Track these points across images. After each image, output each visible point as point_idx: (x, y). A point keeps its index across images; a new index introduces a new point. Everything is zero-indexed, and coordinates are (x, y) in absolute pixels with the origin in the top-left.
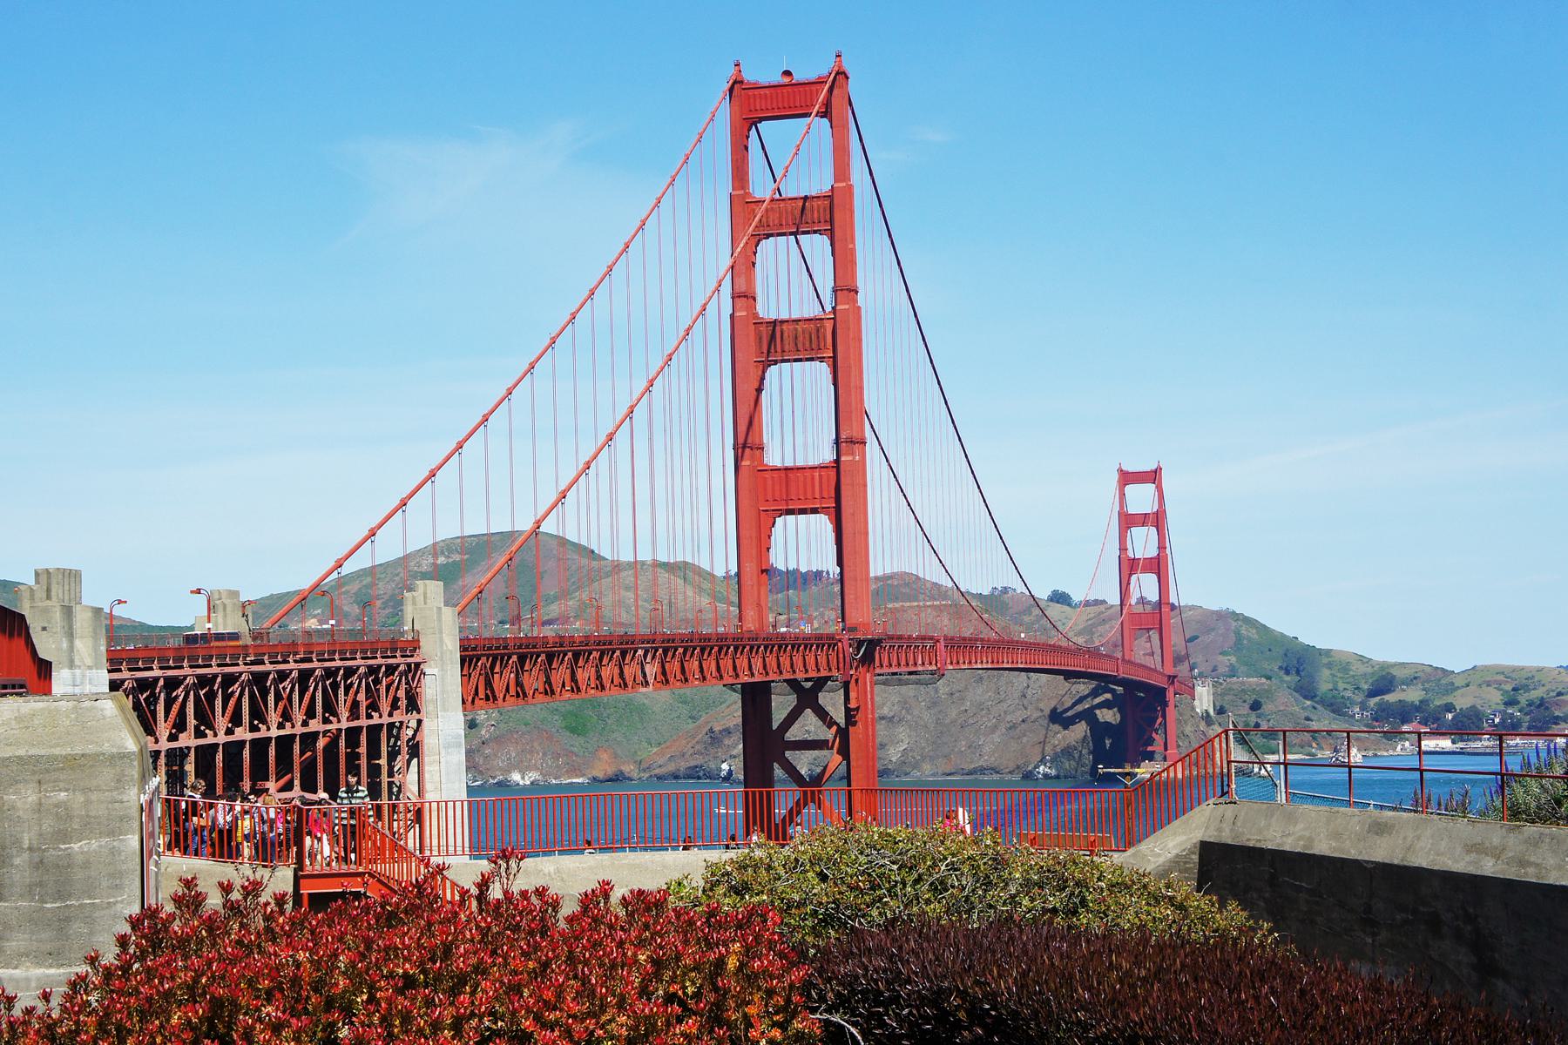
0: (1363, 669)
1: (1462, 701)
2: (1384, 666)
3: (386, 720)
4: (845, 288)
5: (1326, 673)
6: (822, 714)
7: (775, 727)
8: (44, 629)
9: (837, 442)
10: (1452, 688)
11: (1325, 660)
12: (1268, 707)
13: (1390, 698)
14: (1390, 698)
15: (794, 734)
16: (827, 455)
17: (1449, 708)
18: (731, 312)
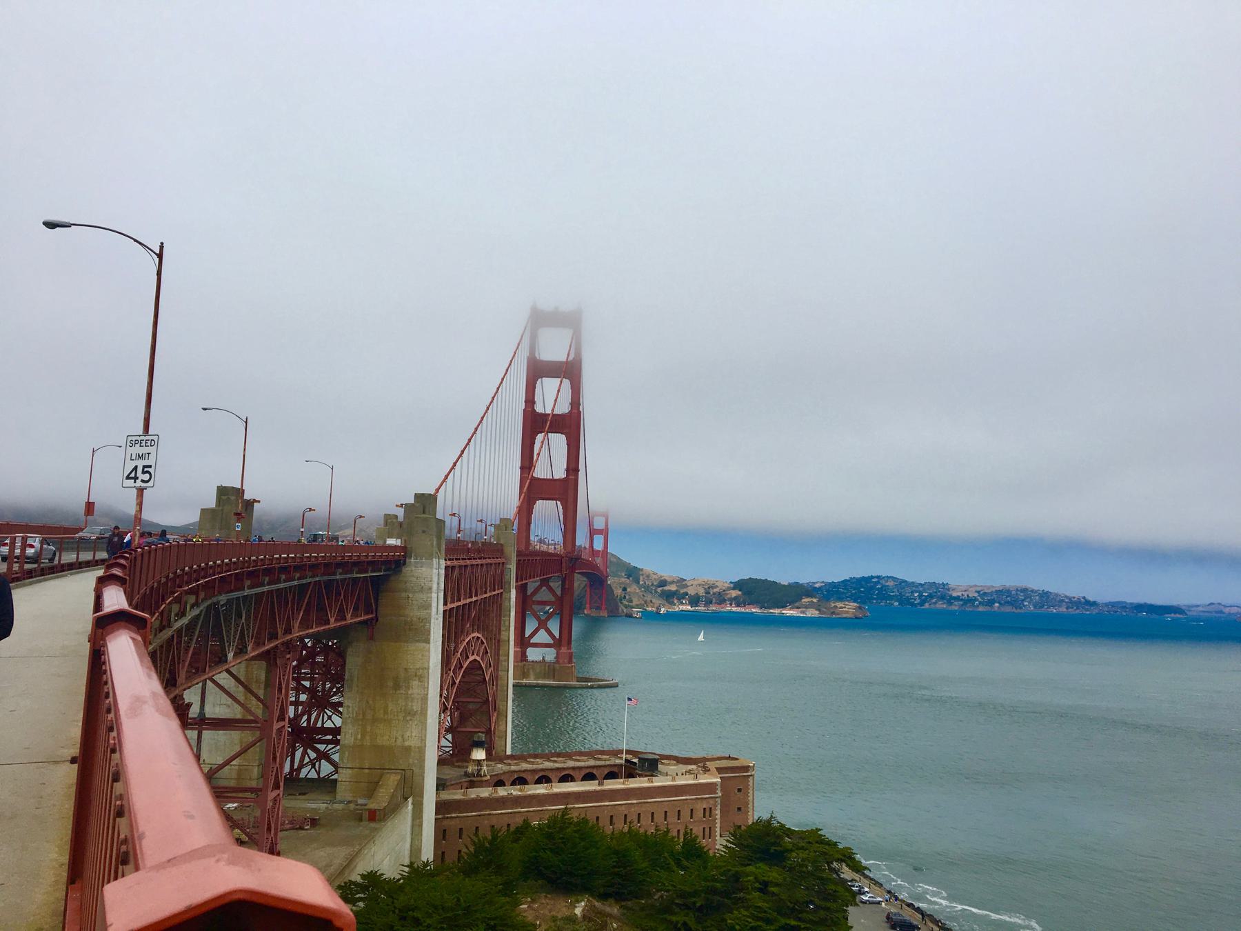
0: (654, 577)
1: (691, 591)
2: (661, 577)
3: (496, 592)
4: (576, 402)
5: (641, 578)
6: (551, 589)
7: (529, 593)
8: (424, 532)
9: (568, 470)
10: (686, 586)
11: (641, 573)
12: (628, 590)
13: (666, 588)
14: (666, 588)
15: (537, 598)
16: (560, 473)
17: (687, 594)
18: (523, 407)
